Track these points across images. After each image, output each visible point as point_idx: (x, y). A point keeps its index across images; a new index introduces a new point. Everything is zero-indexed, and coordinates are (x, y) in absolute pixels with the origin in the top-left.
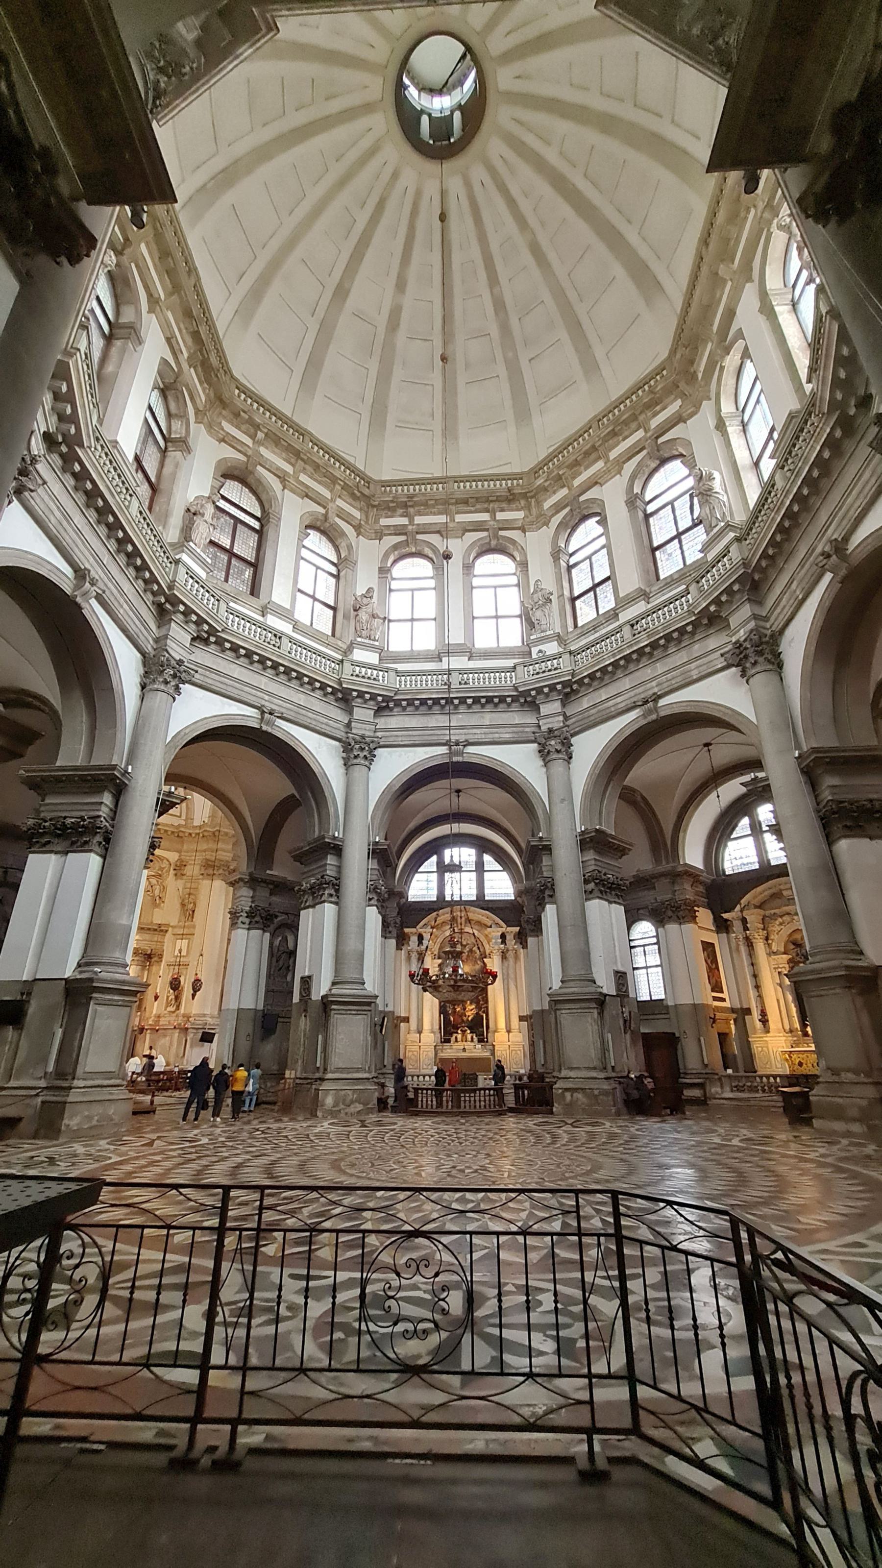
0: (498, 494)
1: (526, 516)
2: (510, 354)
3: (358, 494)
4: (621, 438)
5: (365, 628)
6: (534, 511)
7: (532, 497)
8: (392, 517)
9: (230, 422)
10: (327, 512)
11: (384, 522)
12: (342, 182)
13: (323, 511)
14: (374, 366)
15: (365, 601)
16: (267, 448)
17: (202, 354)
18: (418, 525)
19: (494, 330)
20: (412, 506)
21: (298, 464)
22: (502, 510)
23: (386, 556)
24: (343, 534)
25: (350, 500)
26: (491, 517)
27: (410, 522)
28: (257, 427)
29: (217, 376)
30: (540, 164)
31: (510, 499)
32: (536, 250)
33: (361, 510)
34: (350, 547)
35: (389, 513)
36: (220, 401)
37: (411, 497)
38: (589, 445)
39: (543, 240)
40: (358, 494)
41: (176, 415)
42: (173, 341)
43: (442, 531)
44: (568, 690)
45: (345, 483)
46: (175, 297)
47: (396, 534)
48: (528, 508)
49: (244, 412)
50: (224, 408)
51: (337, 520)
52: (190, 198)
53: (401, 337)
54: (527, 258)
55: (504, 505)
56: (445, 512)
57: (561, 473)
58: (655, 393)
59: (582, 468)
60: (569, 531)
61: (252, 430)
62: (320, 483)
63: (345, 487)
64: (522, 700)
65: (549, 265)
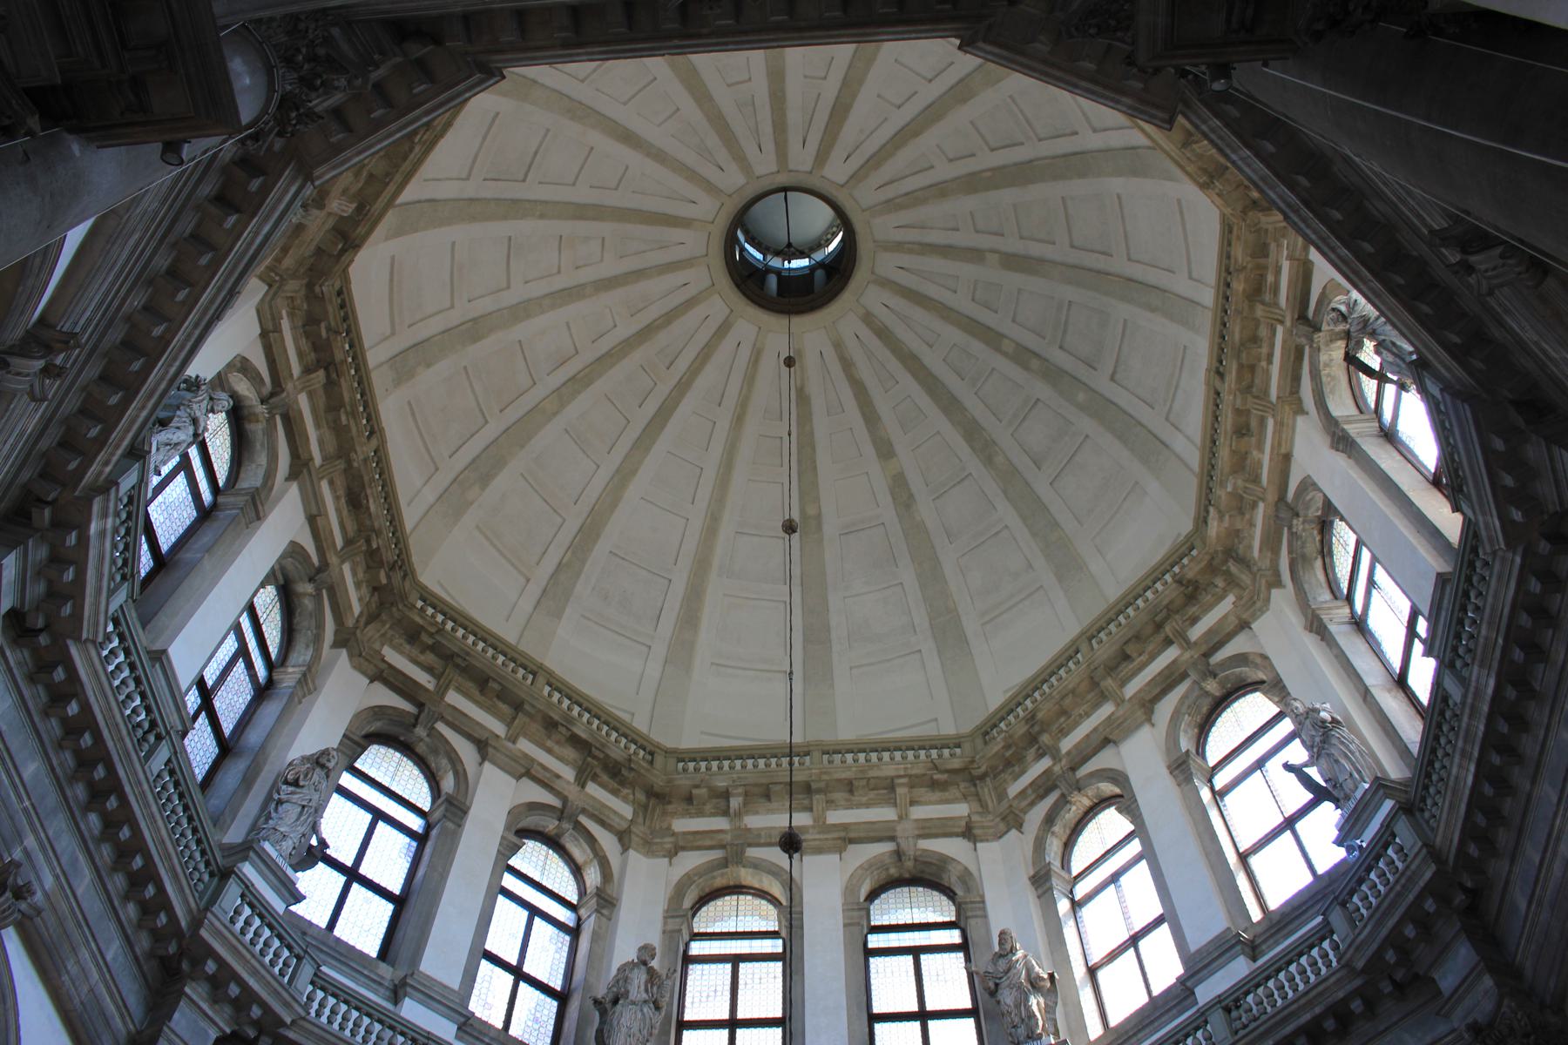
0: (1165, 603)
1: (1239, 598)
2: (1081, 397)
3: (944, 777)
4: (1264, 364)
5: (1017, 1020)
6: (1245, 578)
7: (1226, 562)
8: (1023, 772)
9: (687, 814)
10: (898, 845)
11: (1014, 789)
12: (739, 420)
13: (887, 847)
14: (908, 575)
15: (1002, 964)
16: (757, 813)
17: (595, 757)
18: (1069, 753)
19: (1042, 390)
20: (1042, 731)
21: (815, 802)
22: (1194, 620)
23: (1040, 846)
24: (944, 861)
25: (937, 795)
26: (1182, 647)
27: (1054, 758)
28: (726, 795)
29: (631, 769)
30: (941, 190)
31: (1193, 594)
32: (1013, 262)
33: (965, 797)
34: (966, 877)
35: (1016, 769)
36: (656, 799)
37: (1031, 718)
38: (1230, 415)
39: (1013, 245)
40: (944, 777)
41: (586, 863)
42: (536, 771)
43: (1105, 740)
44: (1459, 899)
45: (910, 776)
46: (521, 719)
47: (1042, 797)
48: (1232, 582)
49: (697, 787)
50: (669, 803)
51: (925, 844)
52: (544, 591)
53: (925, 509)
54: (1016, 279)
55: (1193, 610)
56: (1103, 697)
57: (1229, 489)
58: (1245, 268)
59: (1255, 453)
60: (1318, 563)
61: (722, 803)
62: (867, 805)
63: (914, 782)
64: (1387, 987)
65: (1041, 261)
